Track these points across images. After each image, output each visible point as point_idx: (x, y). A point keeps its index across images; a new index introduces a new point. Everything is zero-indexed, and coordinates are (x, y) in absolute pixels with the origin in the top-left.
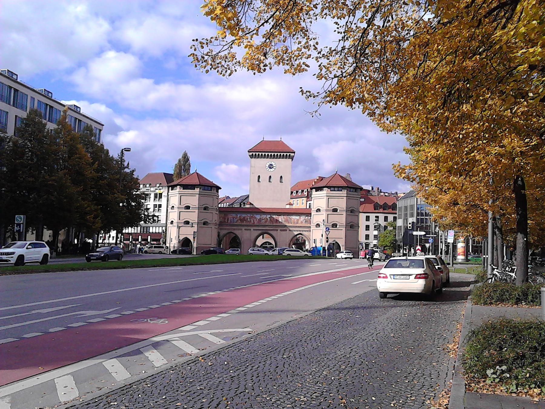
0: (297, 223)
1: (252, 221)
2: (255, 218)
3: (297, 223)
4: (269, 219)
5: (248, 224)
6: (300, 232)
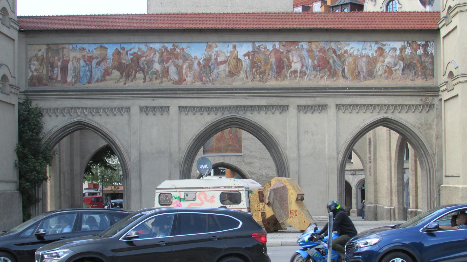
0: (371, 74)
1: (172, 70)
2: (186, 58)
3: (371, 74)
4: (246, 61)
5: (156, 84)
6: (382, 115)
